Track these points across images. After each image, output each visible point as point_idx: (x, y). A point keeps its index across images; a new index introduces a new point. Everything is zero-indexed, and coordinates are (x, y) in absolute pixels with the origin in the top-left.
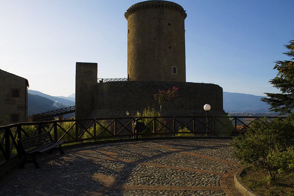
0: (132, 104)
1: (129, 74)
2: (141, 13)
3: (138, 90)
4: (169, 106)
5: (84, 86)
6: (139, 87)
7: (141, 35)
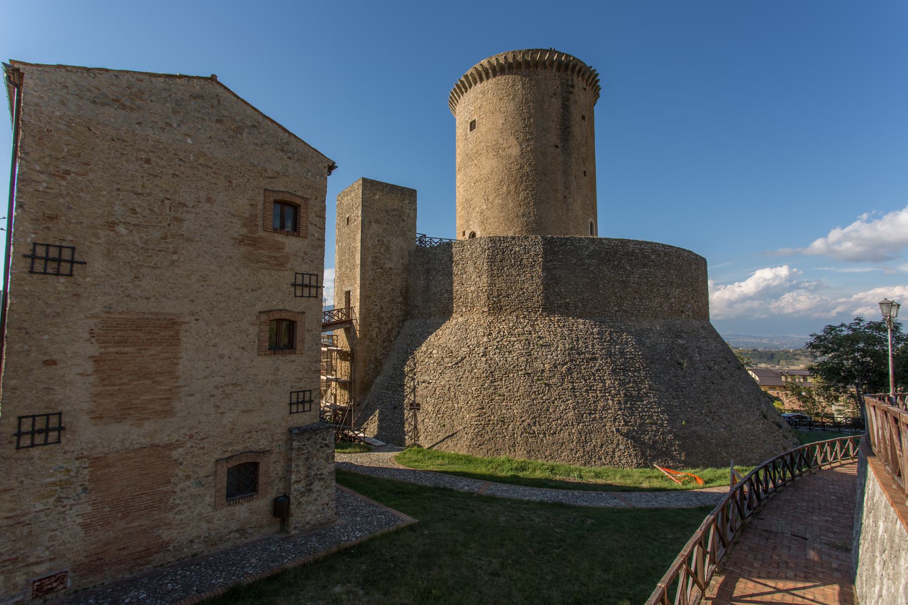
0: (568, 300)
3: (587, 261)
5: (382, 250)
6: (587, 253)
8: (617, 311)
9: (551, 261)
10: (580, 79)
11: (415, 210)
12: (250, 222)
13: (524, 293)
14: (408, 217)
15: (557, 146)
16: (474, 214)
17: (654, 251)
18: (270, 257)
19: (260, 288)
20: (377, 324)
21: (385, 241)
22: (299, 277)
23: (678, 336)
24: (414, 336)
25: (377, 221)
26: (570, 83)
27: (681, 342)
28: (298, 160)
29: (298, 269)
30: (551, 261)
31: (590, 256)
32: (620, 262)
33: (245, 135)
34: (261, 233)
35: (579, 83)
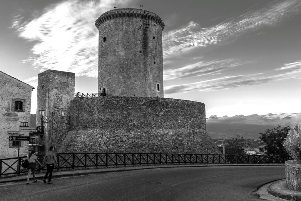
0: (134, 123)
1: (104, 90)
2: (124, 21)
3: (142, 107)
4: (173, 124)
5: (58, 100)
6: (142, 103)
7: (125, 45)
8: (154, 127)
9: (127, 107)
10: (153, 21)
11: (74, 82)
12: (8, 109)
13: (117, 120)
14: (71, 85)
15: (141, 52)
16: (105, 81)
17: (171, 102)
18: (13, 118)
19: (10, 128)
20: (55, 133)
21: (59, 96)
22: (22, 124)
23: (179, 136)
24: (72, 138)
25: (56, 88)
26: (147, 24)
27: (180, 138)
28: (23, 88)
29: (22, 121)
30: (127, 107)
31: (143, 105)
32: (156, 107)
33: (7, 84)
34: (11, 112)
35: (152, 23)
